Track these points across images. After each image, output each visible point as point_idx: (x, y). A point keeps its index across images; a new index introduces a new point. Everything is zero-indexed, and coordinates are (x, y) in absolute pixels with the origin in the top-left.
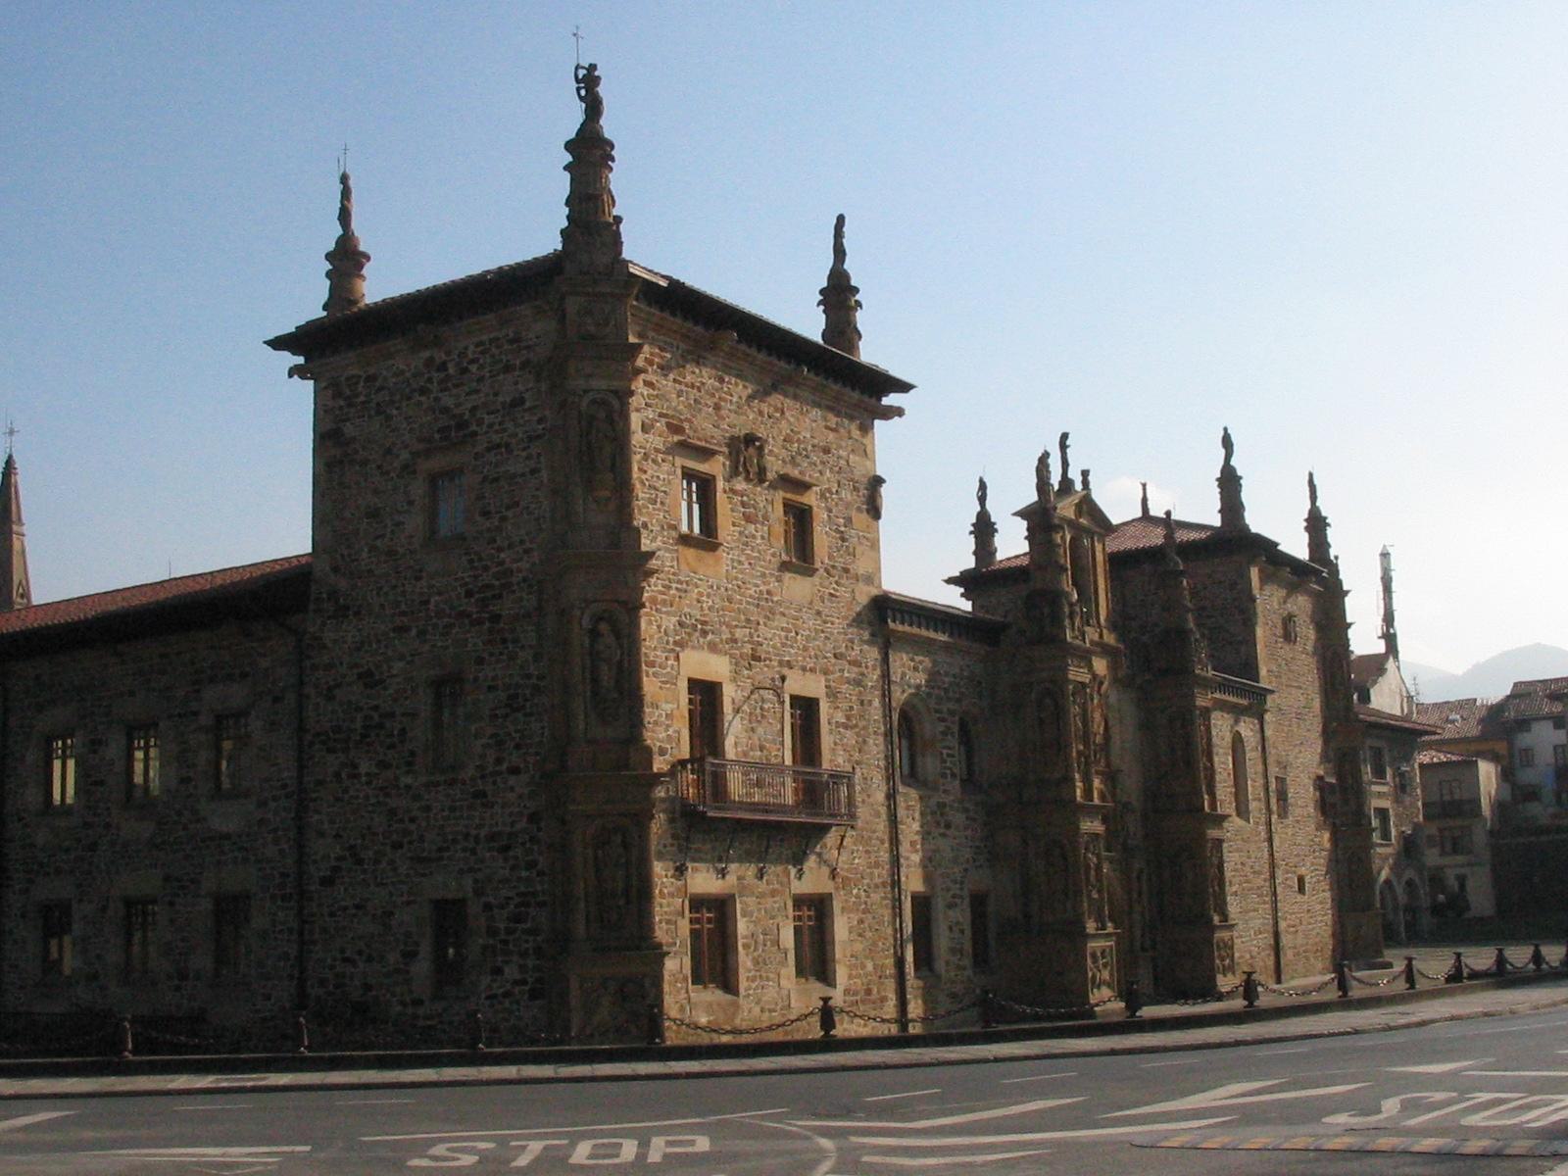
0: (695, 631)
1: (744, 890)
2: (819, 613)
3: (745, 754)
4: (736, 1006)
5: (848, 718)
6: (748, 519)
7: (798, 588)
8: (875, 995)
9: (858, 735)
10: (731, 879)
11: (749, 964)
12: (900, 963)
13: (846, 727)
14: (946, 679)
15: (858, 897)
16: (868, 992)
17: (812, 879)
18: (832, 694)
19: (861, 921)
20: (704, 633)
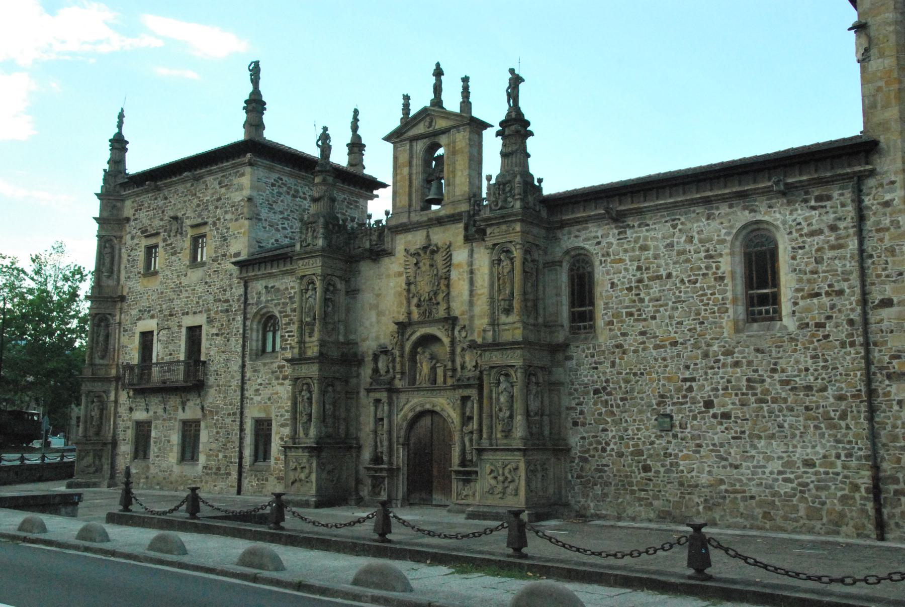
0: (147, 312)
1: (157, 418)
2: (206, 283)
3: (163, 358)
4: (148, 467)
5: (219, 330)
6: (174, 254)
7: (195, 275)
8: (222, 472)
9: (225, 337)
10: (151, 413)
11: (156, 450)
12: (241, 457)
13: (217, 335)
14: (292, 291)
15: (217, 420)
16: (219, 469)
17: (191, 412)
18: (210, 321)
19: (218, 433)
20: (149, 311)
